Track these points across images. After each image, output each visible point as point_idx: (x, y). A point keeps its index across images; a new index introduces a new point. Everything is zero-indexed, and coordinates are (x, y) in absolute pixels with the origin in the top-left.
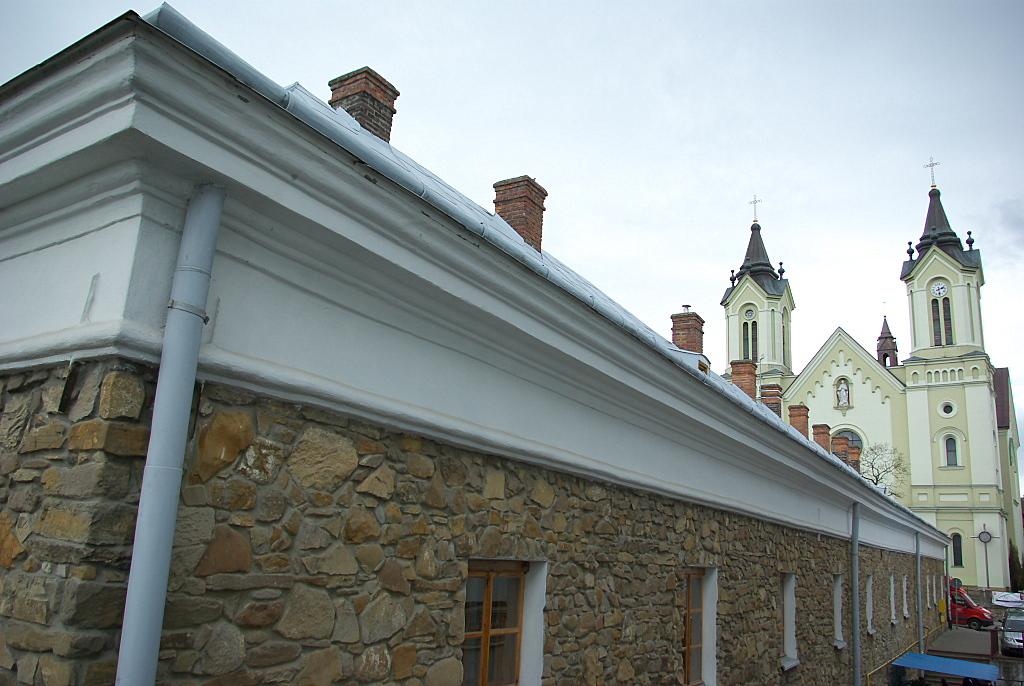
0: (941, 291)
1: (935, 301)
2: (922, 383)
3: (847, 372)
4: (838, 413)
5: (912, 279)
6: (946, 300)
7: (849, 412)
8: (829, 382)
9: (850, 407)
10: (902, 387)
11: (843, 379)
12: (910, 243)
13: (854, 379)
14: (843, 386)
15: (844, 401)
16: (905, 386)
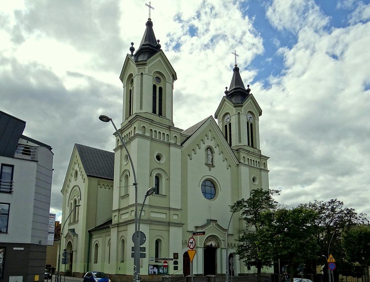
0: (251, 119)
1: (248, 123)
2: (247, 163)
3: (212, 144)
4: (207, 168)
5: (242, 106)
6: (251, 124)
7: (212, 169)
8: (203, 147)
9: (214, 166)
10: (238, 163)
11: (209, 148)
12: (227, 88)
13: (216, 150)
14: (209, 152)
15: (210, 163)
16: (240, 162)
